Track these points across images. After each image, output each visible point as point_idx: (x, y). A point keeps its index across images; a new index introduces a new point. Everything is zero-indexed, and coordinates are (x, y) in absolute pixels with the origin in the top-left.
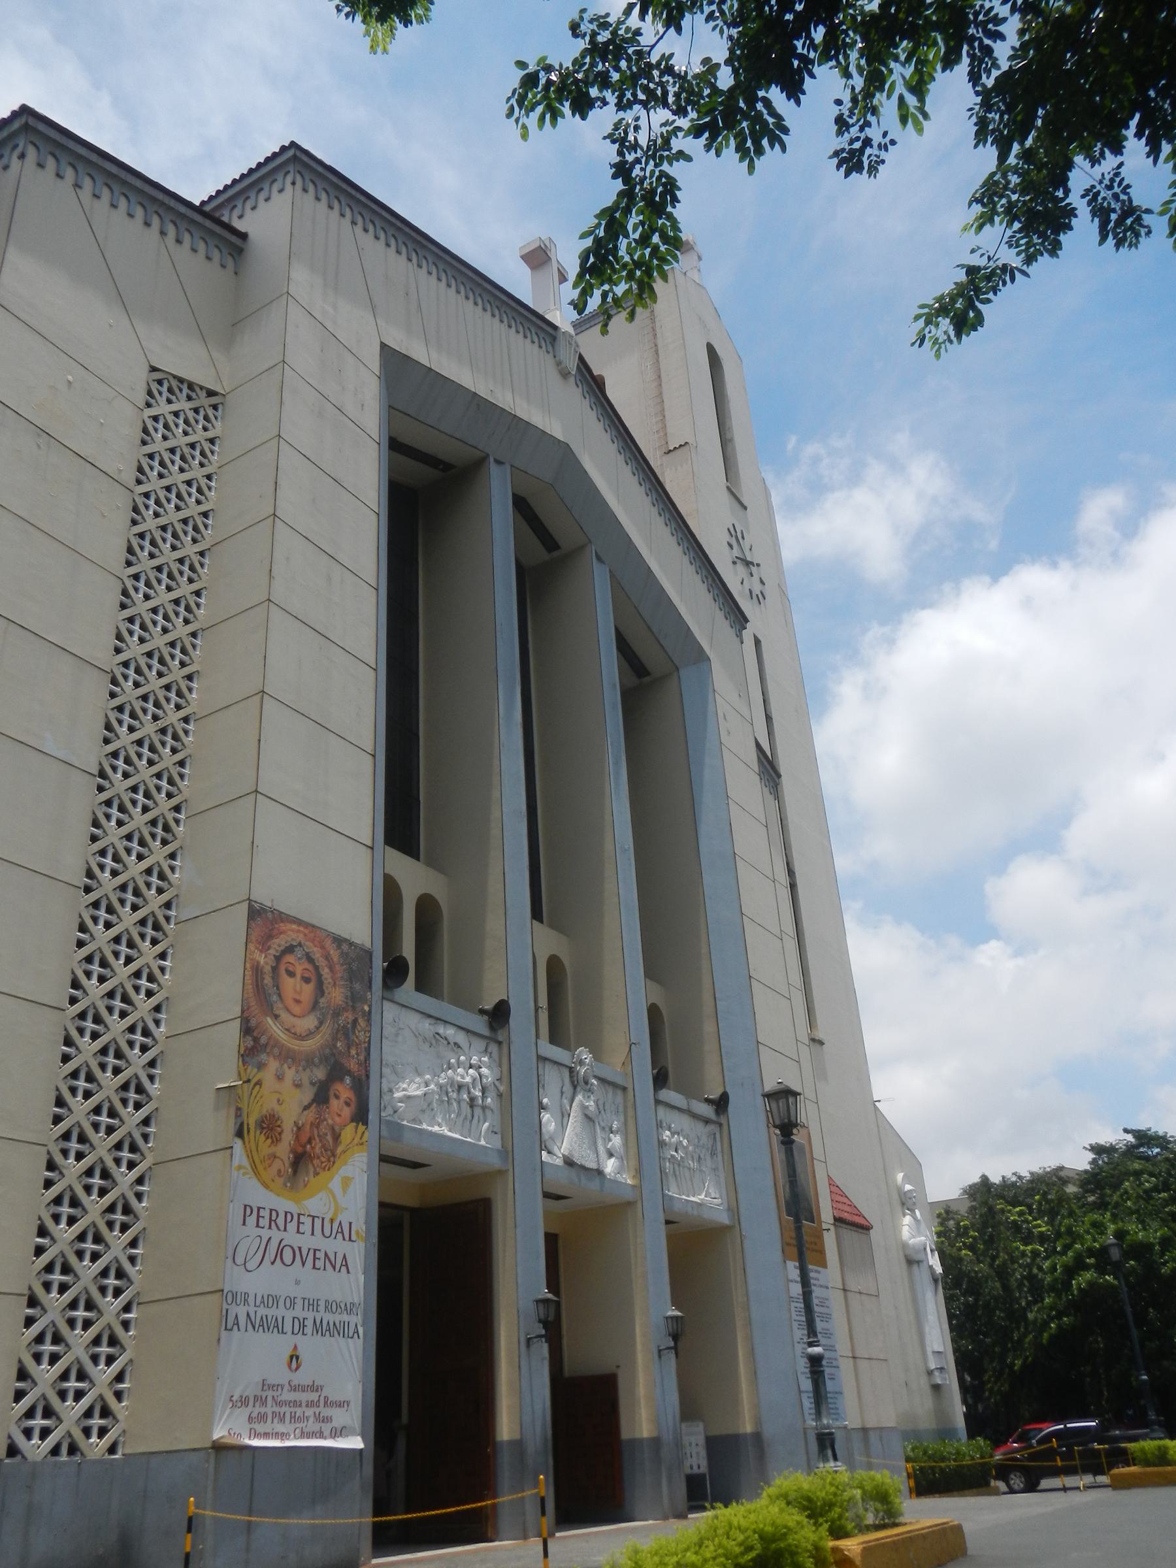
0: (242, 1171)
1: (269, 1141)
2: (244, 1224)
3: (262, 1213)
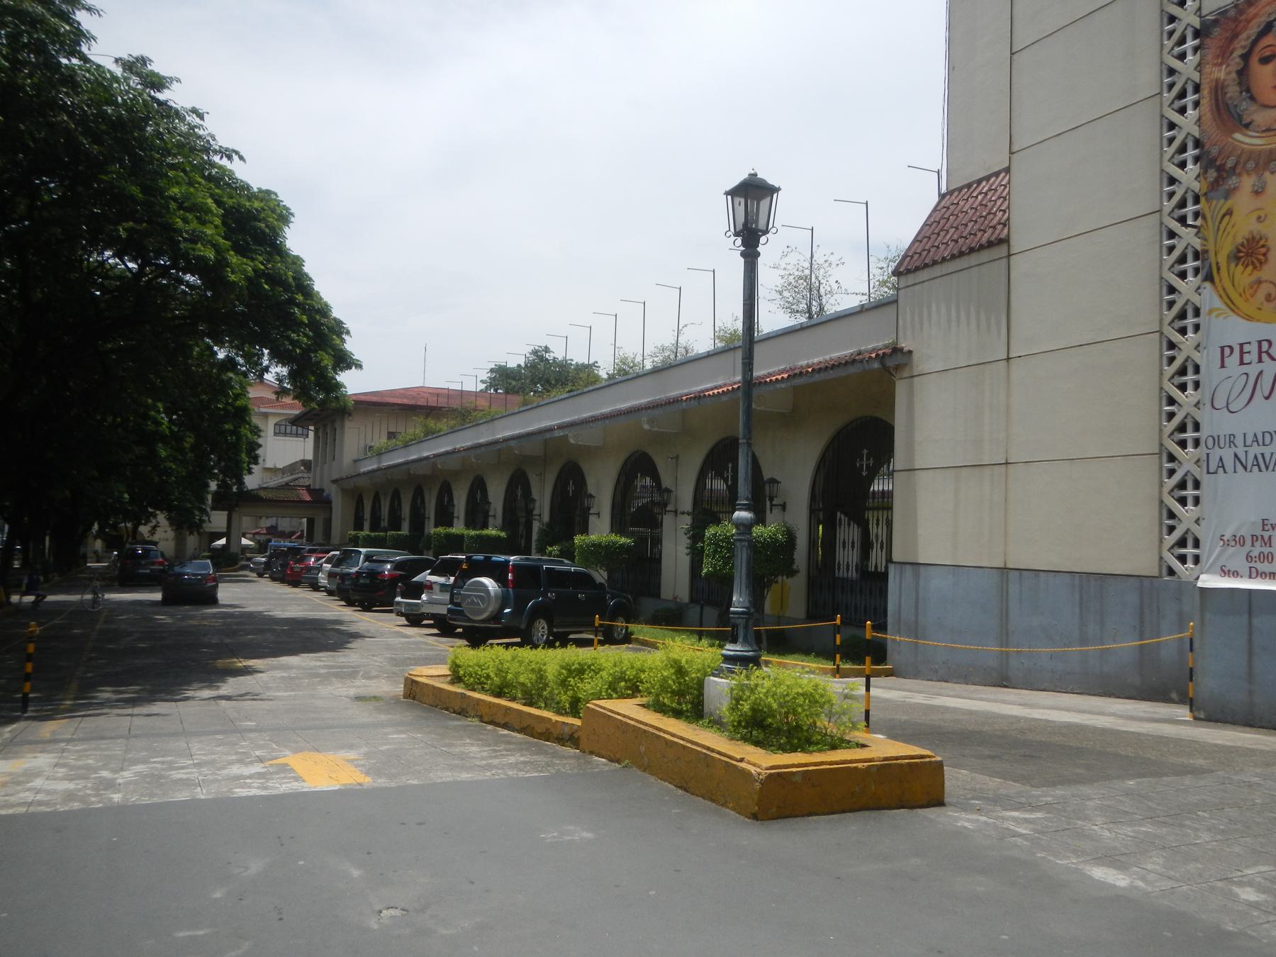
0: (1214, 314)
1: (1250, 268)
2: (1223, 366)
3: (1246, 348)
